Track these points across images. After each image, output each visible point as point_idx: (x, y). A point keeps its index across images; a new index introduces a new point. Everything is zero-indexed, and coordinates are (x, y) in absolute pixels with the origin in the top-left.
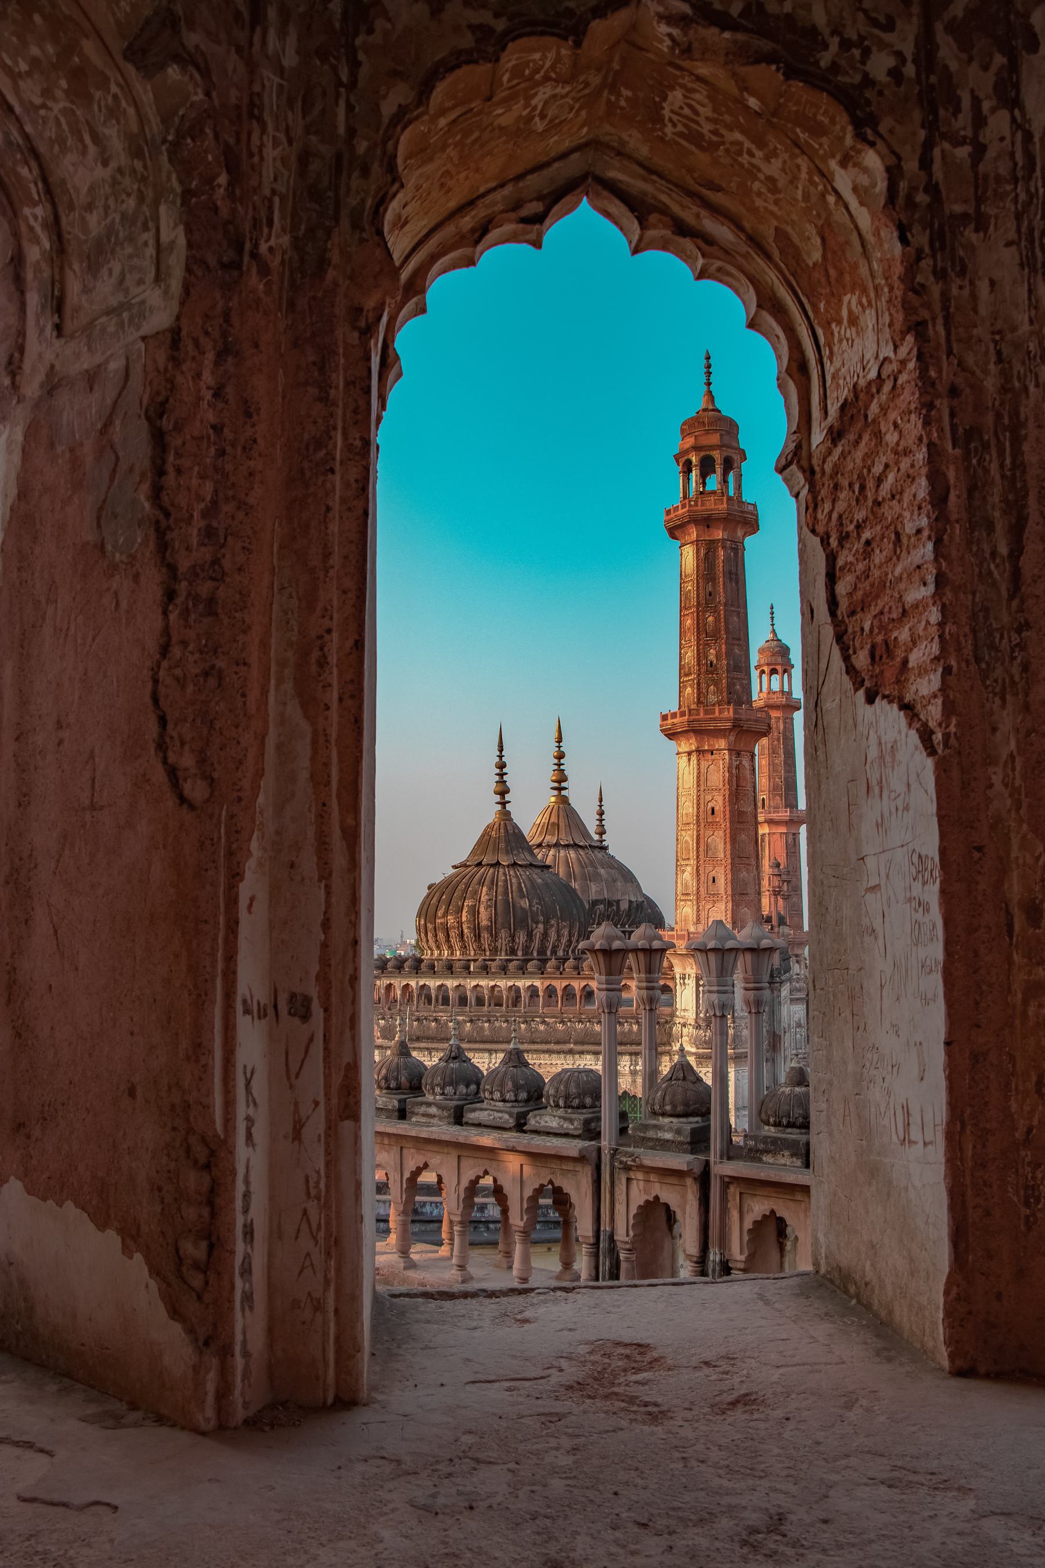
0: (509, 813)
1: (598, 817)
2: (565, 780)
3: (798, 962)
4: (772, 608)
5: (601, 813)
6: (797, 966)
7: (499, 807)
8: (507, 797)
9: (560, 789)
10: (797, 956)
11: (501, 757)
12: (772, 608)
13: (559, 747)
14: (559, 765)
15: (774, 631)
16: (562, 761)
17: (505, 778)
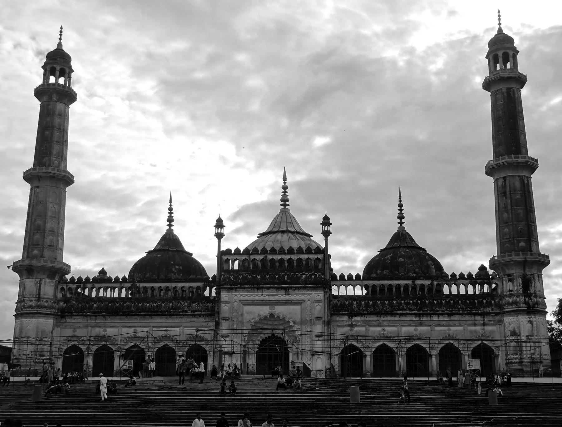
0: (172, 230)
1: (399, 208)
2: (288, 201)
3: (510, 280)
4: (499, 12)
5: (400, 206)
6: (510, 284)
7: (168, 227)
8: (172, 223)
9: (285, 205)
10: (509, 275)
11: (171, 205)
12: (499, 12)
13: (285, 183)
14: (285, 192)
15: (500, 30)
16: (286, 190)
17: (172, 215)
